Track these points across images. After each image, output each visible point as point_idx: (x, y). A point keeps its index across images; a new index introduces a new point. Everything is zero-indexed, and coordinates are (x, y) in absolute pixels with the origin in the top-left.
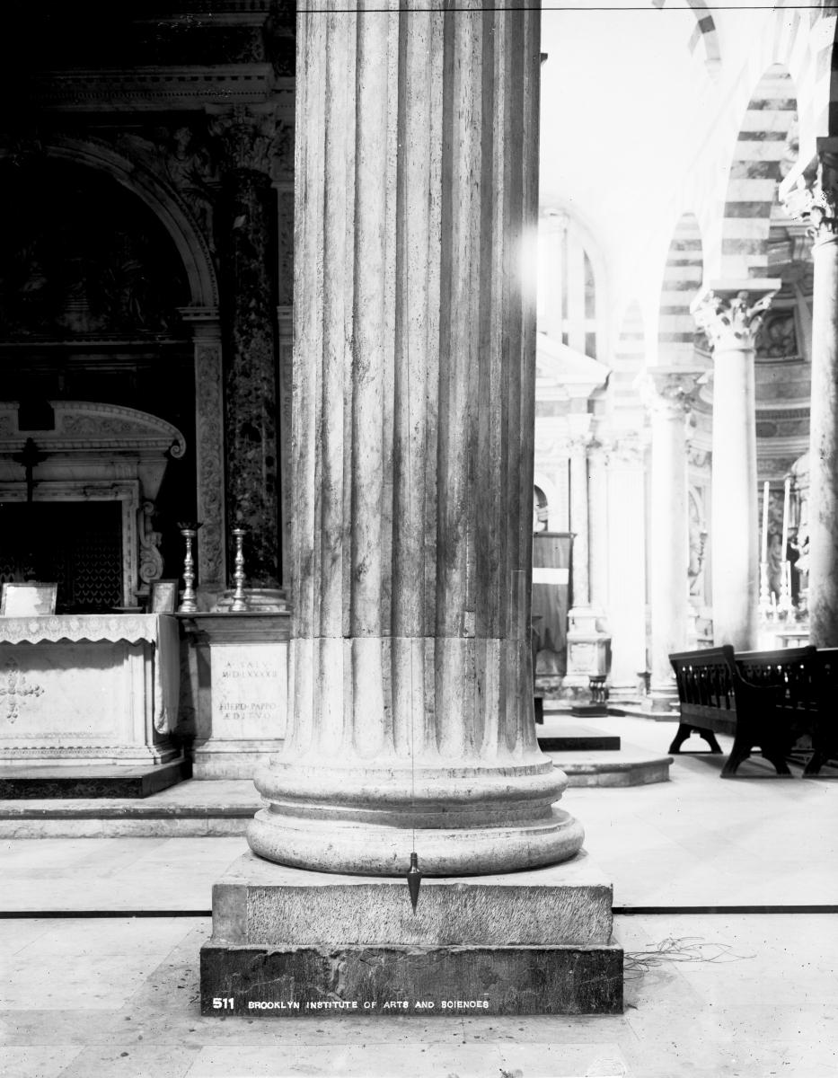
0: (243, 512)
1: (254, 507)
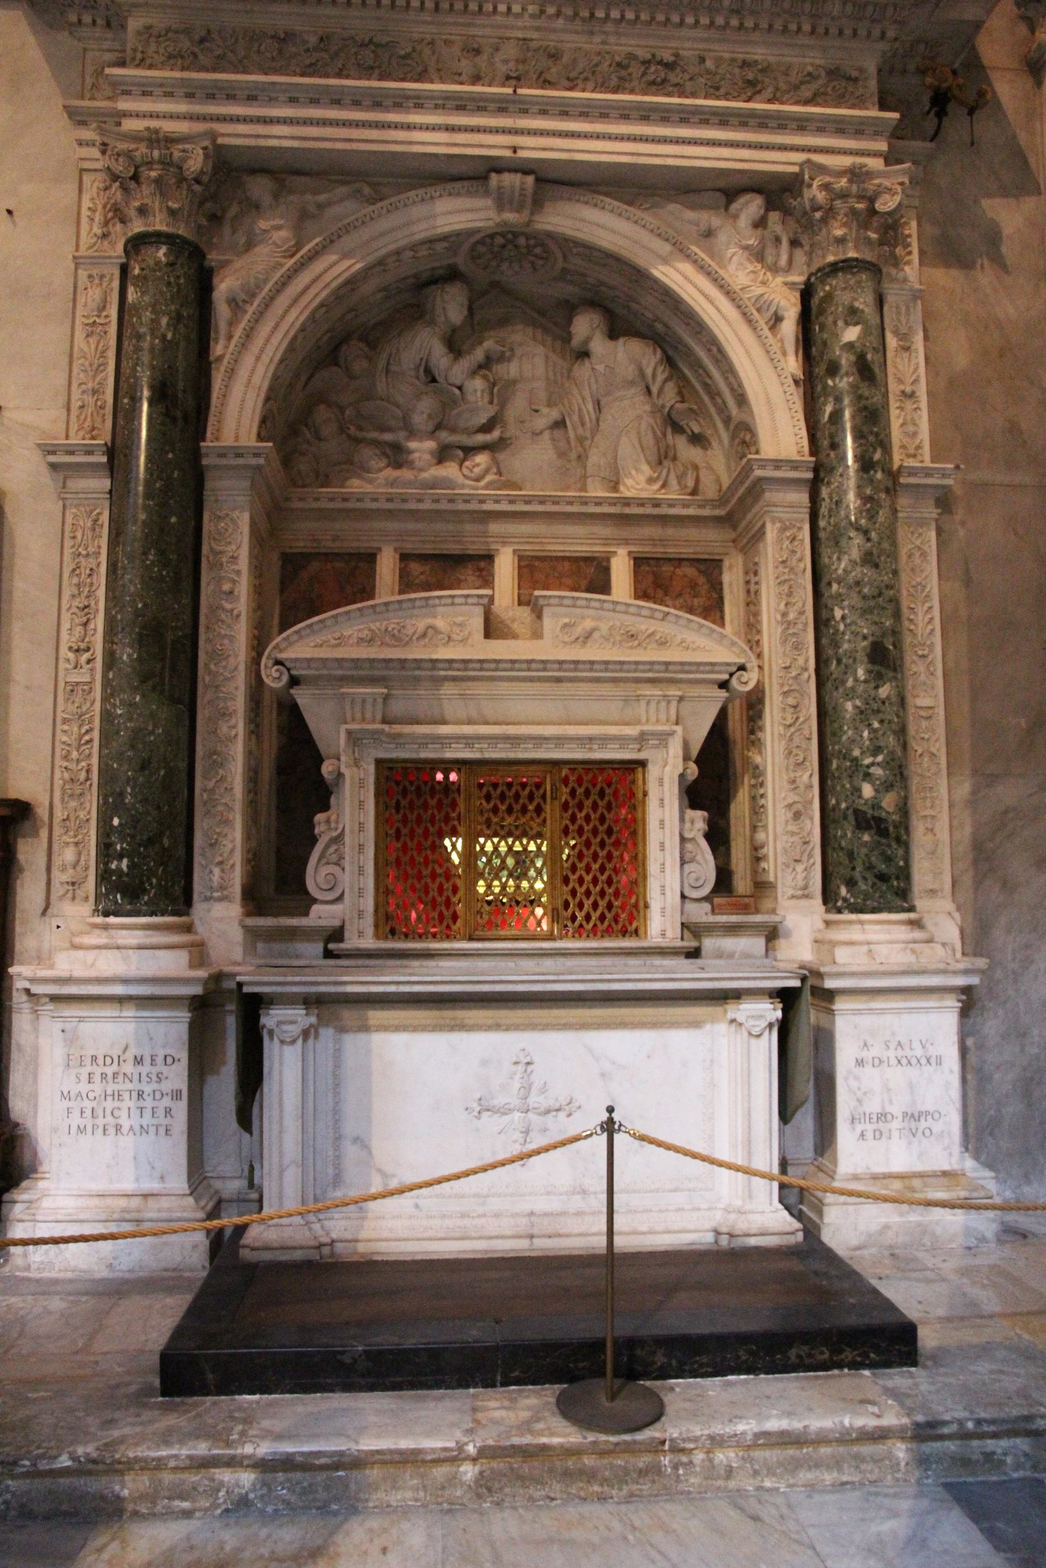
0: (873, 785)
1: (891, 778)
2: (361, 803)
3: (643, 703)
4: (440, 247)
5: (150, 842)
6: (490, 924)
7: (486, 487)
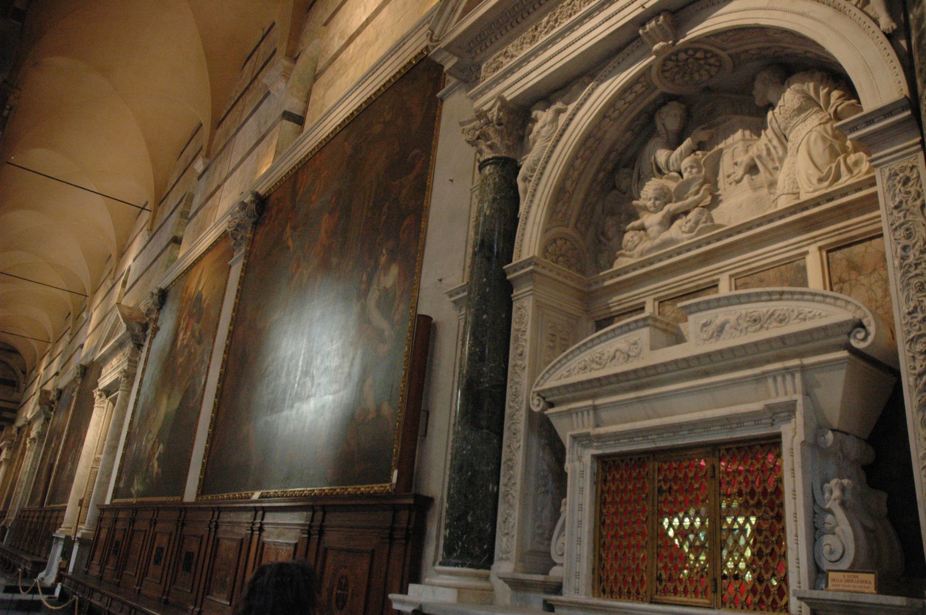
2: (582, 489)
3: (770, 381)
4: (638, 88)
5: (459, 519)
6: (665, 591)
7: (697, 235)
